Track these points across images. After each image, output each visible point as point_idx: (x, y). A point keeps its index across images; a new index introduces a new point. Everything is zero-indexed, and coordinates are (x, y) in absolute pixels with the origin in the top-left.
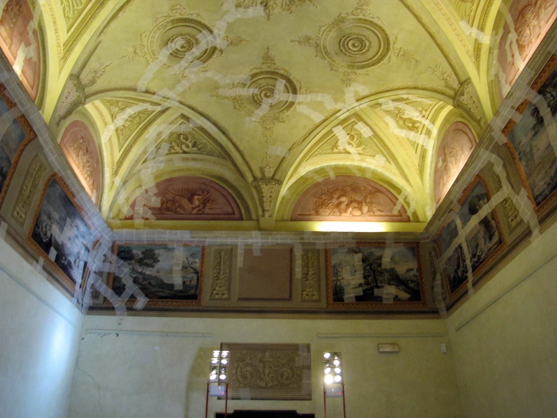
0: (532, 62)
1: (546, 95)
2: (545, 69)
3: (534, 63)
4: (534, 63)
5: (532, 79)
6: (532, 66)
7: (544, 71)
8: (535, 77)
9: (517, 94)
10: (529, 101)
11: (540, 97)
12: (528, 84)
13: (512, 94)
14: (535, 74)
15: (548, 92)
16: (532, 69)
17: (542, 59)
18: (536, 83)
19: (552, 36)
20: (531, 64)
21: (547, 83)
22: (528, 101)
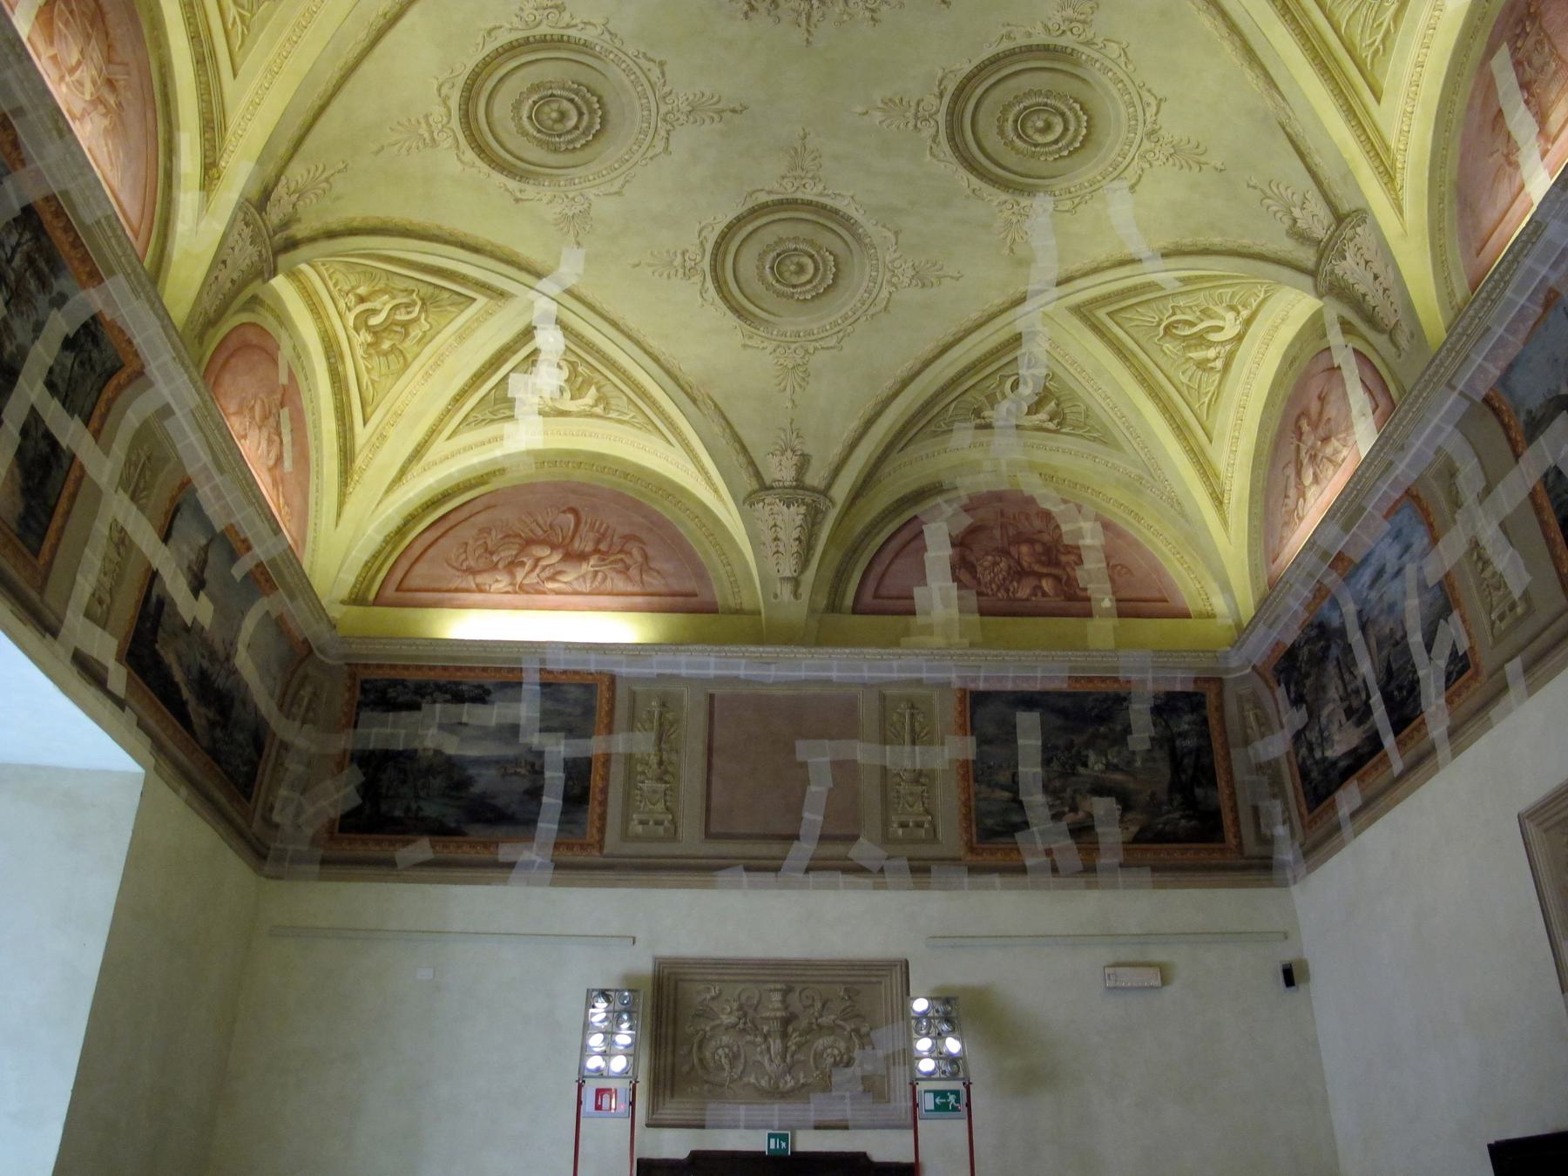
0: (114, 230)
1: (16, 228)
2: (72, 234)
3: (109, 233)
4: (109, 233)
5: (73, 207)
6: (106, 228)
7: (76, 243)
8: (73, 216)
9: (53, 150)
10: (15, 169)
11: (17, 207)
12: (65, 193)
13: (61, 136)
14: (82, 224)
15: (21, 235)
16: (98, 222)
17: (110, 256)
18: (59, 213)
19: (142, 294)
20: (110, 226)
21: (43, 239)
22: (18, 166)
